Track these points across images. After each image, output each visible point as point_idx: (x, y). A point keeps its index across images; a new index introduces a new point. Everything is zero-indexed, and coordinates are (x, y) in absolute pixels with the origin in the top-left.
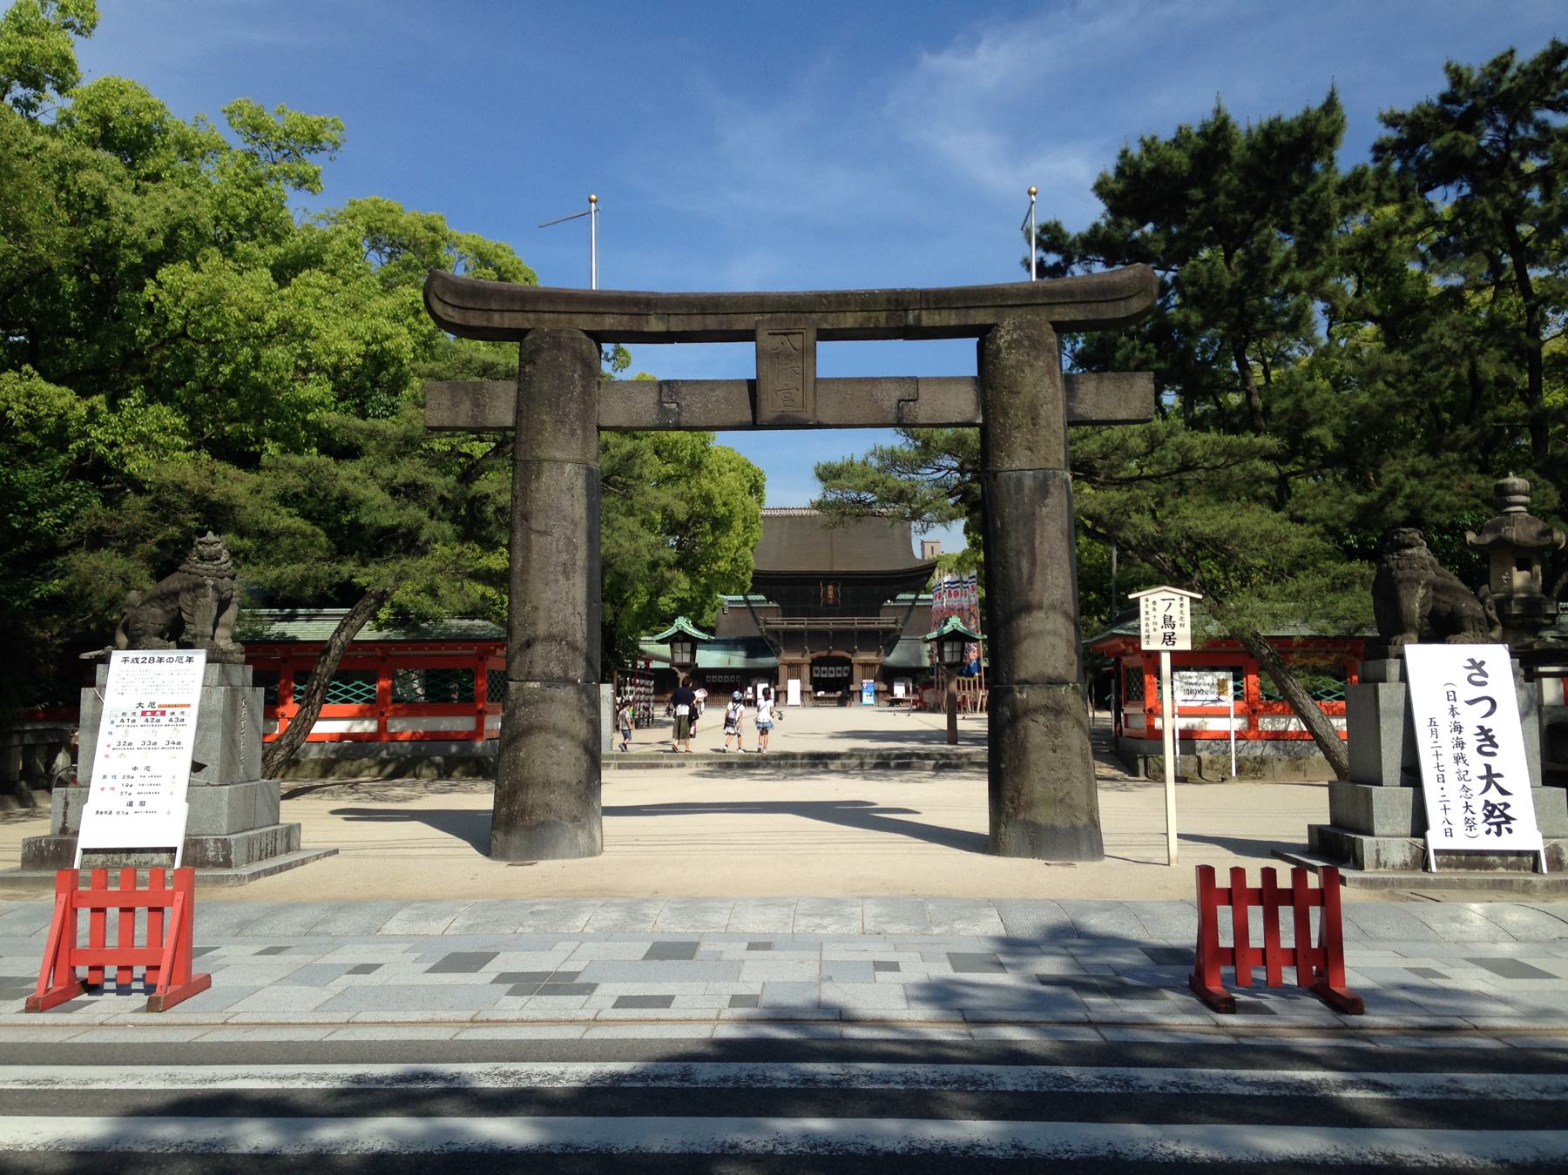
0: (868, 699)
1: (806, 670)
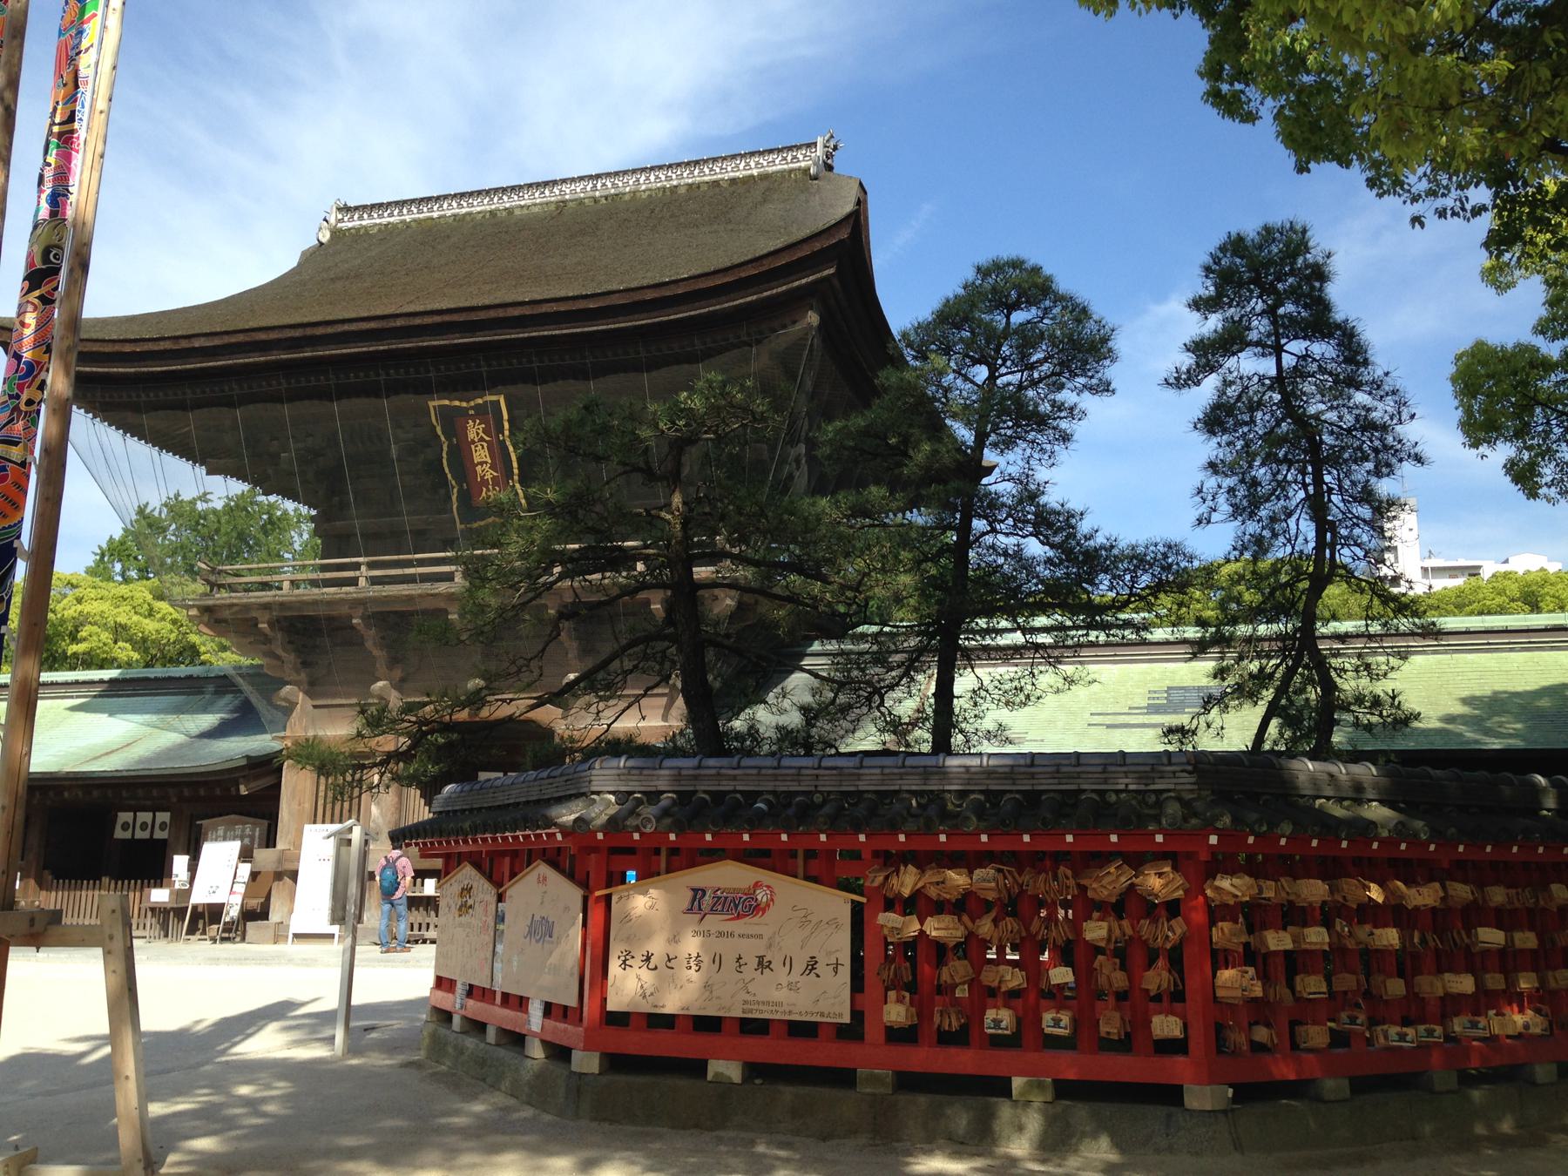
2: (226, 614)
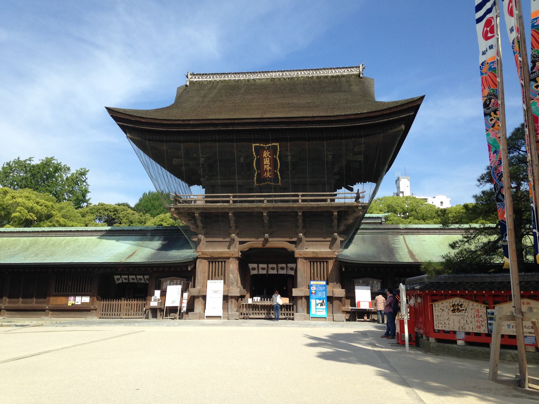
1: (233, 267)
2: (182, 211)
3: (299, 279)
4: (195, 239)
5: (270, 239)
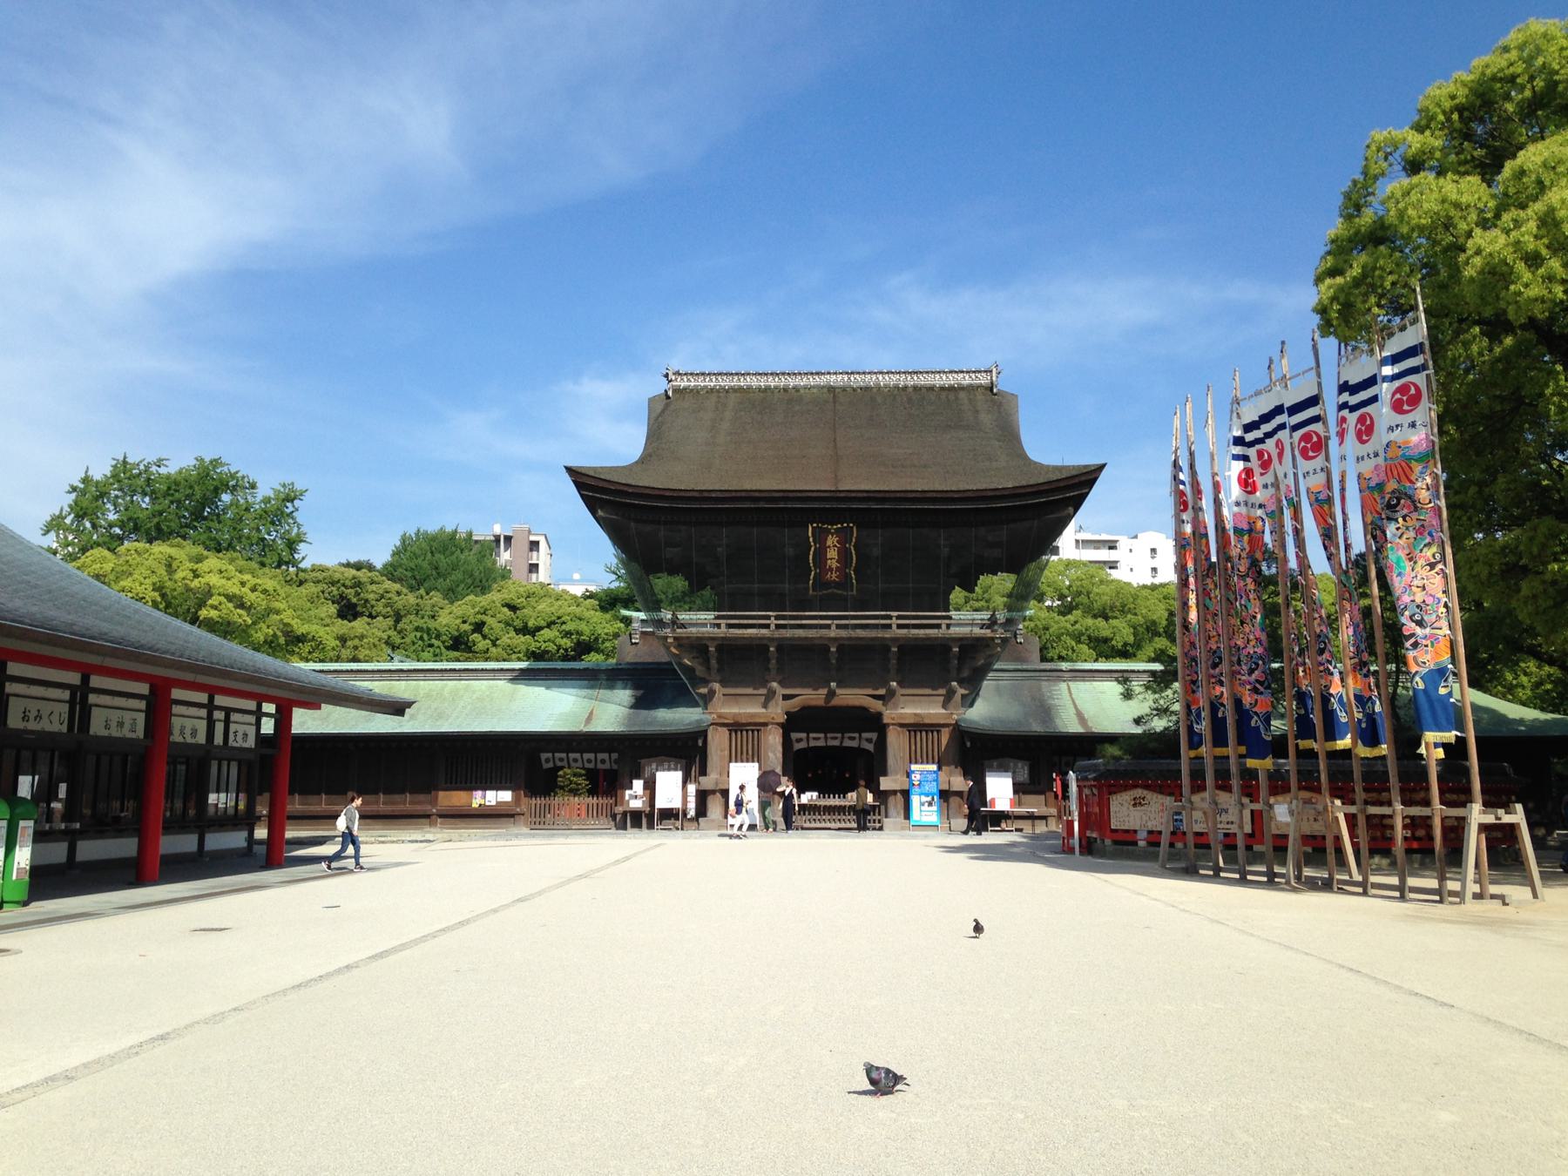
0: (924, 810)
1: (773, 740)
3: (891, 761)
4: (704, 690)
5: (839, 691)
